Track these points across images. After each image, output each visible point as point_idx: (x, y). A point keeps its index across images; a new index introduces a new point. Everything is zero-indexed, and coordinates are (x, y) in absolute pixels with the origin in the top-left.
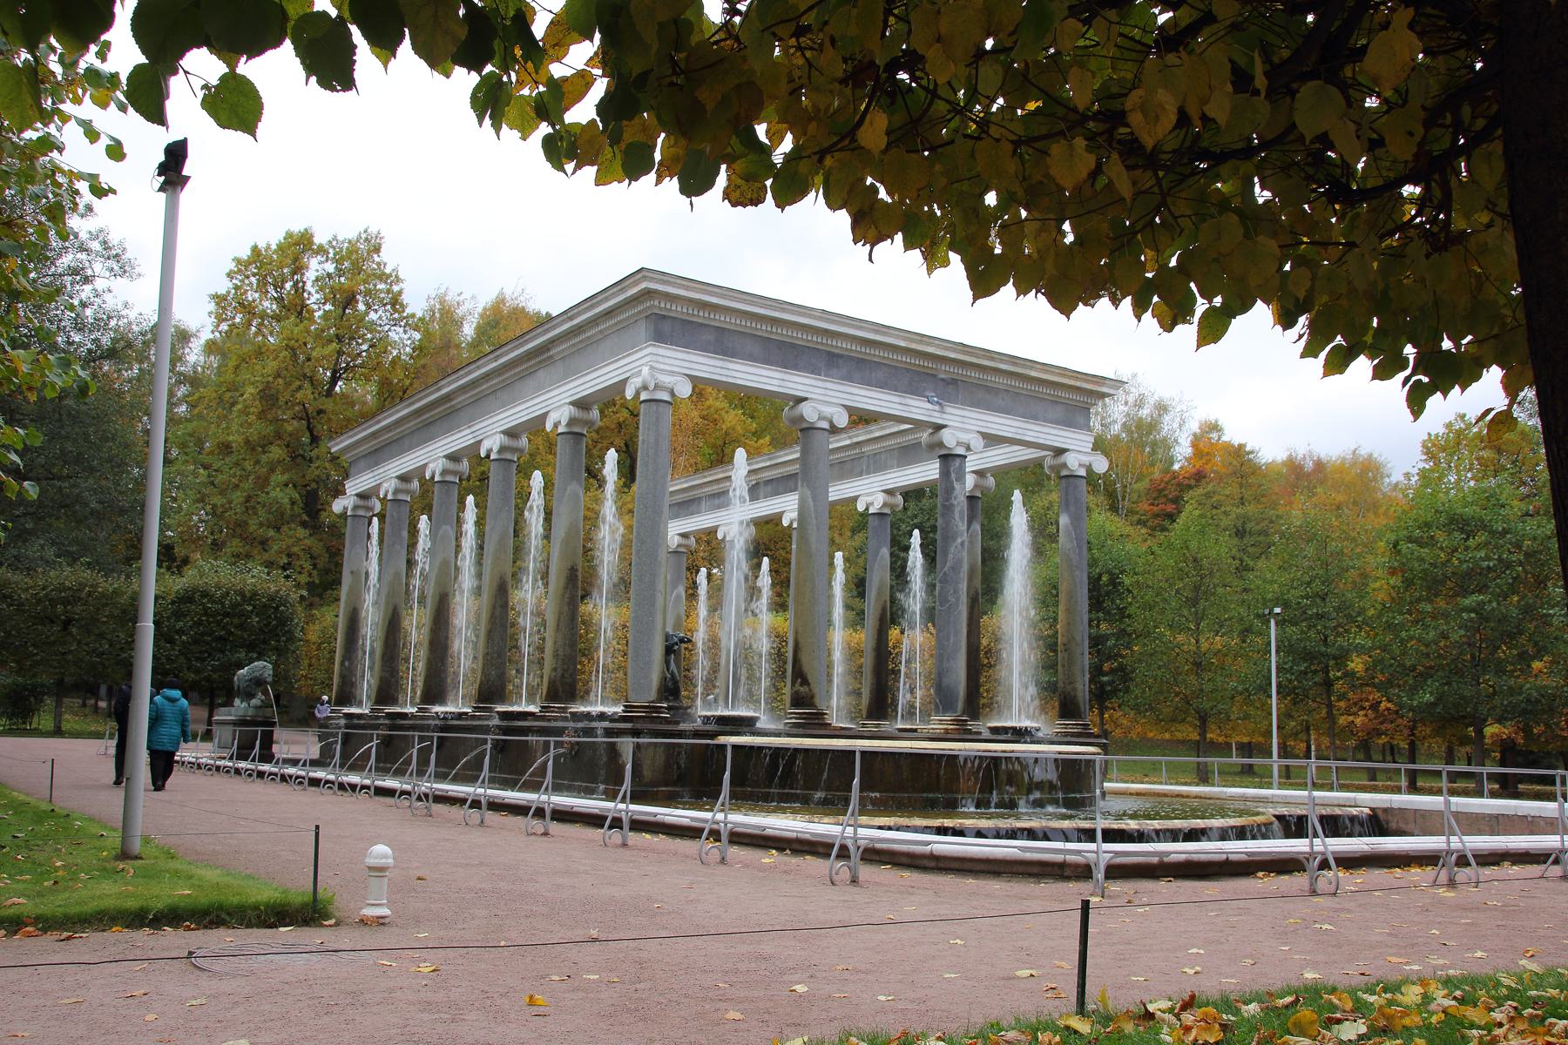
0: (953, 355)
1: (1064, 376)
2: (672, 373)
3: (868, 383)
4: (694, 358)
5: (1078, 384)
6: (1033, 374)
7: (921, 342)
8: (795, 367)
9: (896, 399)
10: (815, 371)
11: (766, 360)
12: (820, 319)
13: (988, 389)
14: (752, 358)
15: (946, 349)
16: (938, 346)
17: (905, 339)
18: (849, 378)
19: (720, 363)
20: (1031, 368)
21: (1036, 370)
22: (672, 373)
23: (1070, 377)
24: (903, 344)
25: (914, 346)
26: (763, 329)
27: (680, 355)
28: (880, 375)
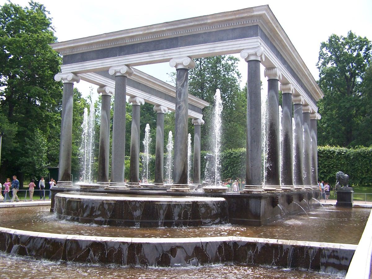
0: (165, 29)
1: (226, 16)
2: (67, 73)
3: (136, 52)
4: (73, 66)
5: (237, 16)
6: (209, 21)
7: (148, 29)
8: (108, 56)
9: (147, 55)
10: (114, 55)
11: (98, 58)
12: (106, 37)
13: (194, 36)
14: (93, 59)
15: (160, 27)
16: (157, 28)
17: (141, 31)
18: (128, 53)
19: (81, 65)
20: (207, 19)
21: (209, 19)
22: (67, 73)
23: (231, 15)
24: (141, 33)
25: (146, 32)
26: (95, 48)
27: (69, 67)
28: (141, 47)
